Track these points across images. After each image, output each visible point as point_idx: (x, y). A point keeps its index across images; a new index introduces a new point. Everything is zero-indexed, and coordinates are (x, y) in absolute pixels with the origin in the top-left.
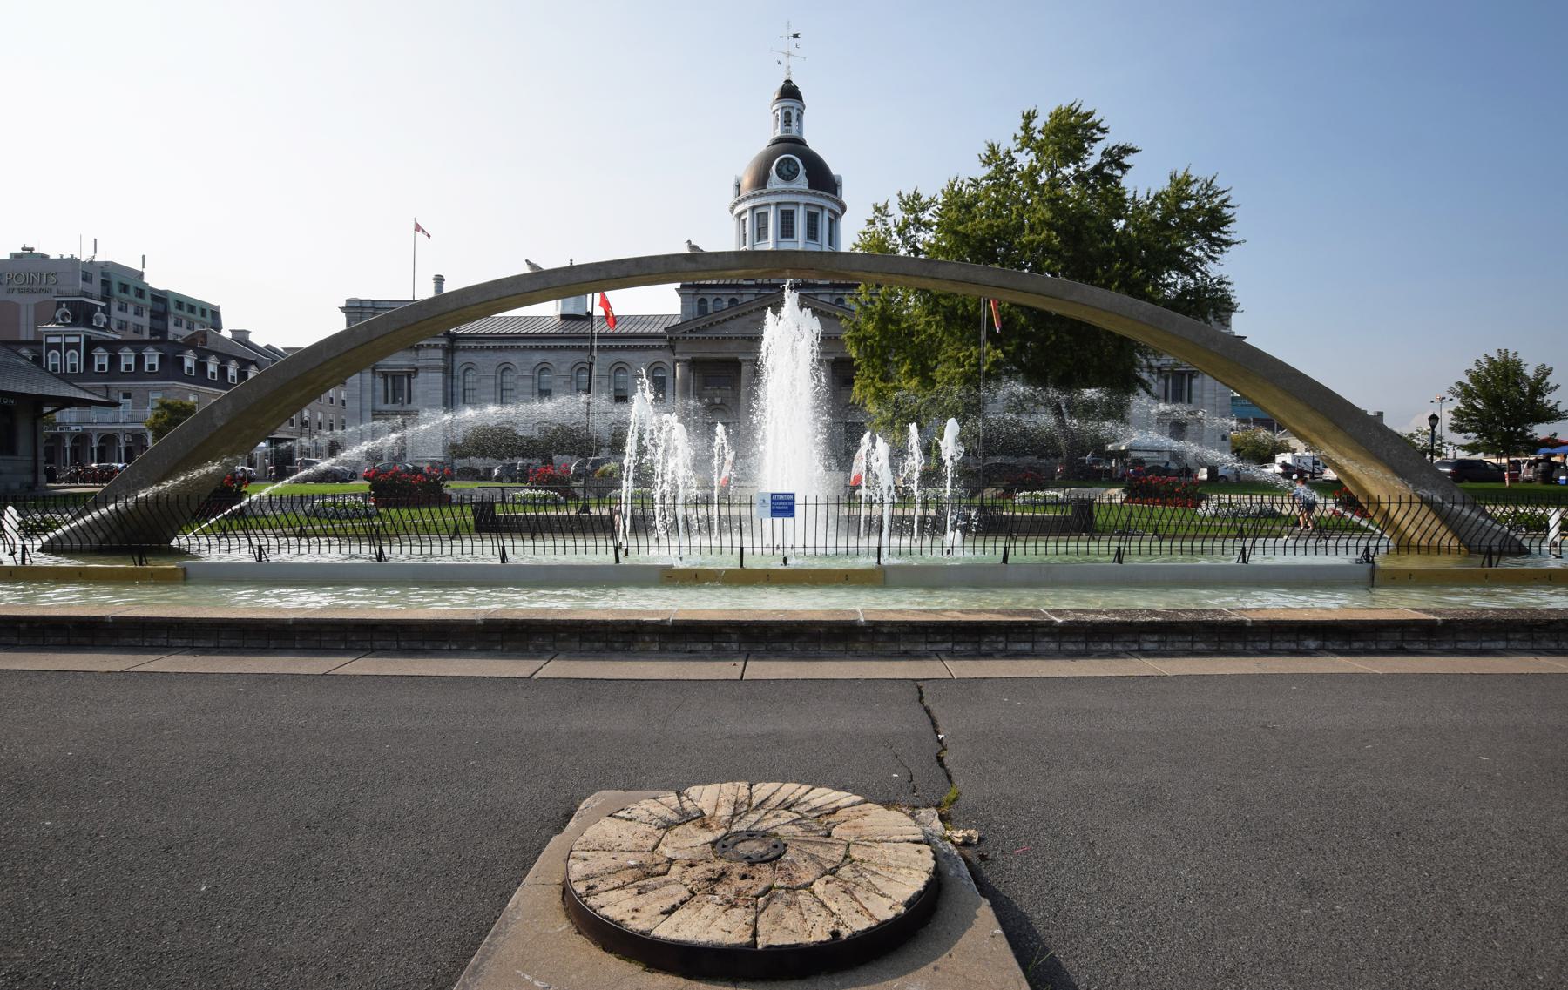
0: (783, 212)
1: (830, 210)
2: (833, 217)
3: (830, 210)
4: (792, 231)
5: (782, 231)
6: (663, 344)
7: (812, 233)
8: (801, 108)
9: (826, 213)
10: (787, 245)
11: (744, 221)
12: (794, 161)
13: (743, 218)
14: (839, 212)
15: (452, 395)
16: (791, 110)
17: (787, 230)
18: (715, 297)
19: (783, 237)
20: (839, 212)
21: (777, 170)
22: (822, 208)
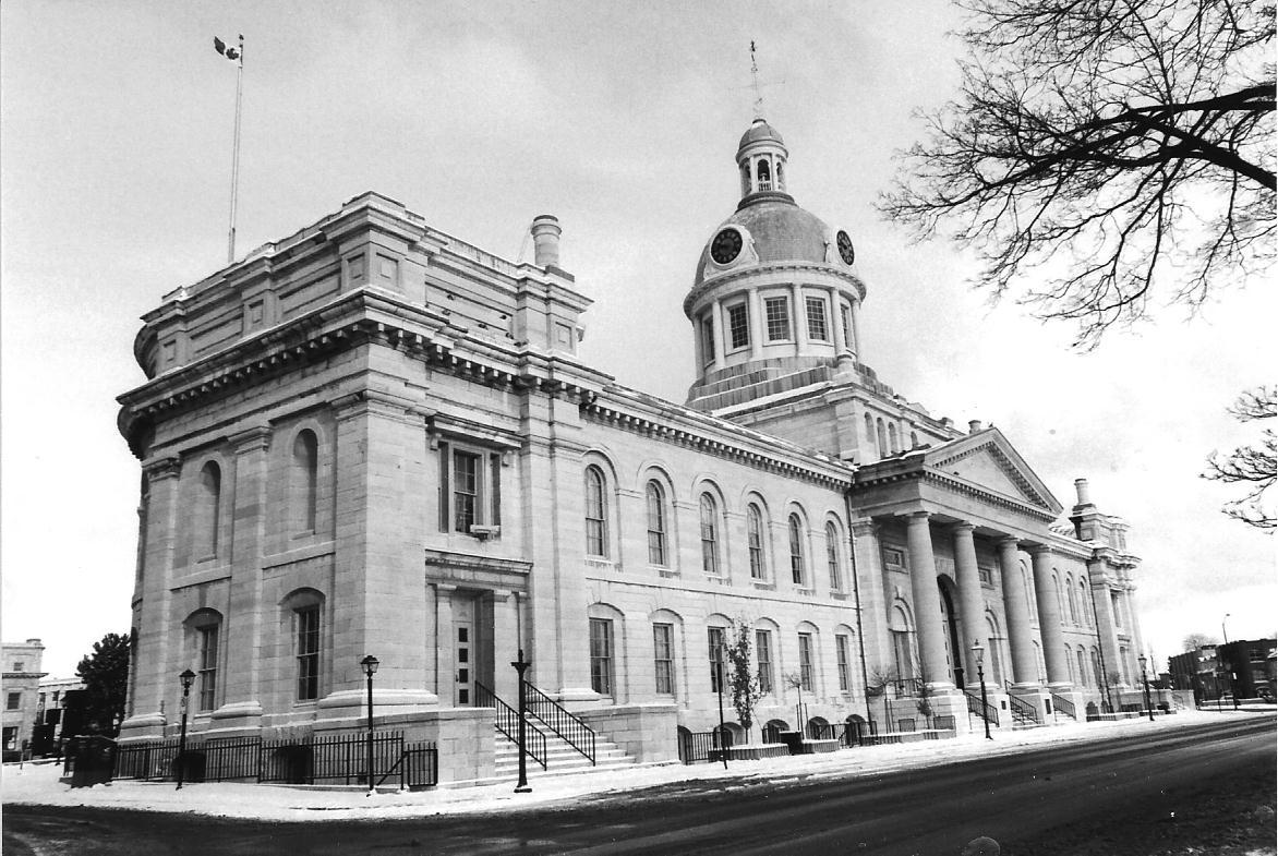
1: (842, 293)
2: (847, 303)
3: (842, 293)
4: (786, 329)
5: (771, 331)
7: (818, 328)
8: (783, 154)
9: (836, 295)
11: (709, 323)
13: (704, 319)
14: (857, 296)
16: (767, 158)
17: (778, 325)
19: (772, 338)
20: (857, 296)
22: (830, 290)
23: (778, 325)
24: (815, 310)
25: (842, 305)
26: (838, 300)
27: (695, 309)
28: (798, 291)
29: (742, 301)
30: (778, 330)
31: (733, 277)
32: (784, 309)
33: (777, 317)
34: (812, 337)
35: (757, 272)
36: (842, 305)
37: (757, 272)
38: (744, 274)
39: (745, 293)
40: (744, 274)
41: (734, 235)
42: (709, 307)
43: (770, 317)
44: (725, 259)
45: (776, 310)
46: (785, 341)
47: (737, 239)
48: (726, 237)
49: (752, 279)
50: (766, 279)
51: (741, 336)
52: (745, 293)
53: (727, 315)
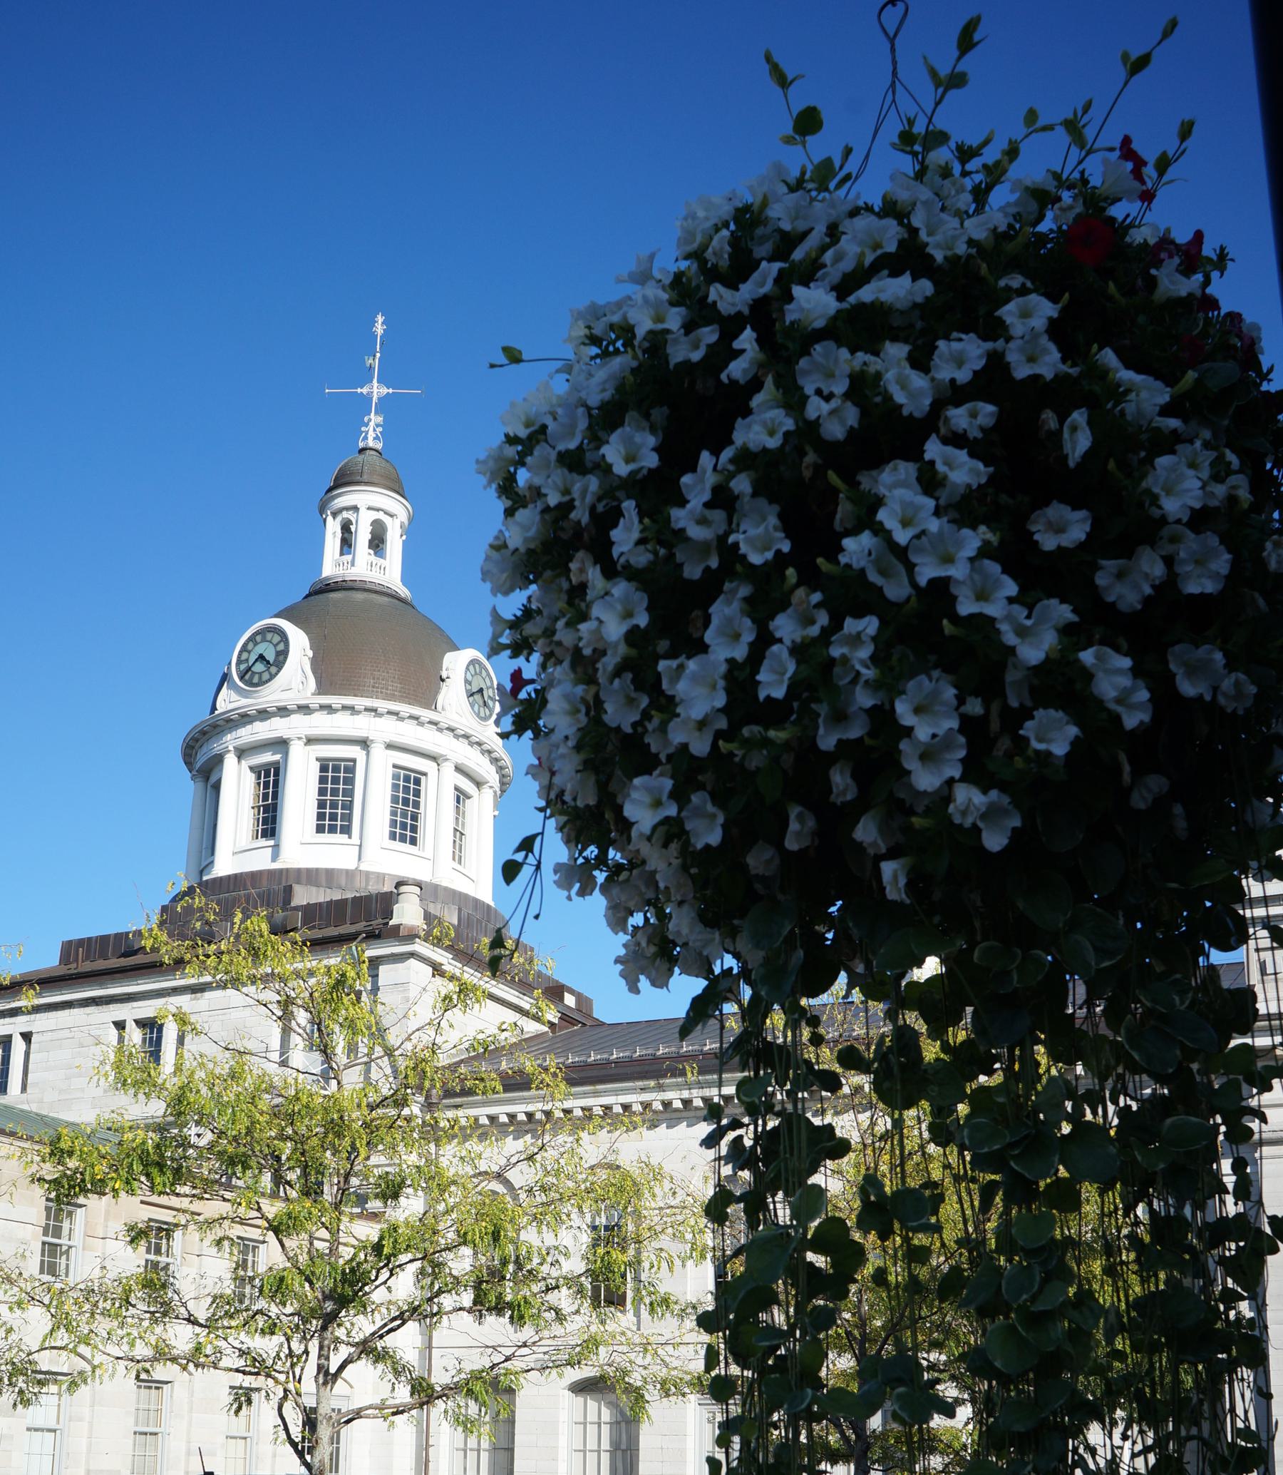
0: (324, 765)
4: (348, 818)
5: (321, 816)
9: (448, 768)
13: (213, 779)
25: (457, 789)
26: (452, 778)
28: (378, 750)
29: (277, 757)
30: (333, 817)
31: (263, 714)
32: (350, 781)
33: (335, 792)
34: (393, 836)
35: (304, 709)
36: (457, 789)
37: (304, 709)
38: (283, 711)
39: (281, 744)
40: (283, 711)
41: (277, 638)
42: (218, 760)
44: (256, 680)
46: (342, 838)
47: (281, 647)
48: (264, 640)
49: (296, 718)
51: (269, 823)
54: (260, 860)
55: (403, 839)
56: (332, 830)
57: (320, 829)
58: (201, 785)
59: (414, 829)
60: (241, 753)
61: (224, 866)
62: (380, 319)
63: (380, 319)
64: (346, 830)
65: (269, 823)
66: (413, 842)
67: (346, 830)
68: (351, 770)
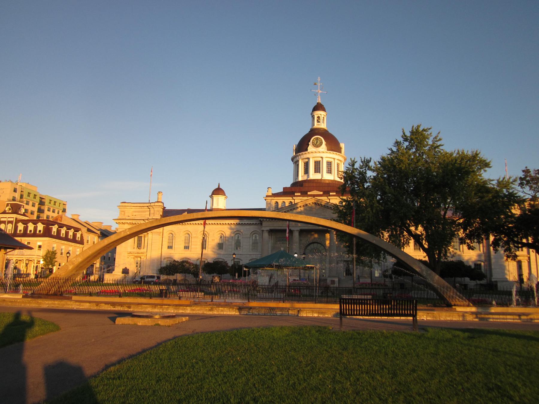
3: (338, 160)
4: (320, 170)
5: (315, 170)
6: (257, 222)
10: (318, 176)
11: (298, 165)
12: (320, 138)
13: (297, 164)
15: (162, 245)
16: (320, 116)
17: (317, 169)
18: (282, 201)
19: (315, 172)
21: (312, 142)
22: (334, 159)
23: (317, 169)
24: (329, 165)
27: (295, 160)
30: (317, 170)
32: (320, 164)
33: (317, 166)
34: (327, 172)
43: (315, 166)
45: (317, 164)
50: (315, 155)
51: (306, 171)
52: (308, 159)
53: (303, 164)
54: (305, 178)
55: (329, 173)
56: (317, 172)
57: (315, 172)
58: (295, 164)
59: (331, 171)
60: (302, 159)
61: (300, 179)
62: (319, 78)
63: (319, 78)
64: (320, 172)
65: (306, 171)
66: (330, 173)
67: (320, 172)
68: (320, 162)
